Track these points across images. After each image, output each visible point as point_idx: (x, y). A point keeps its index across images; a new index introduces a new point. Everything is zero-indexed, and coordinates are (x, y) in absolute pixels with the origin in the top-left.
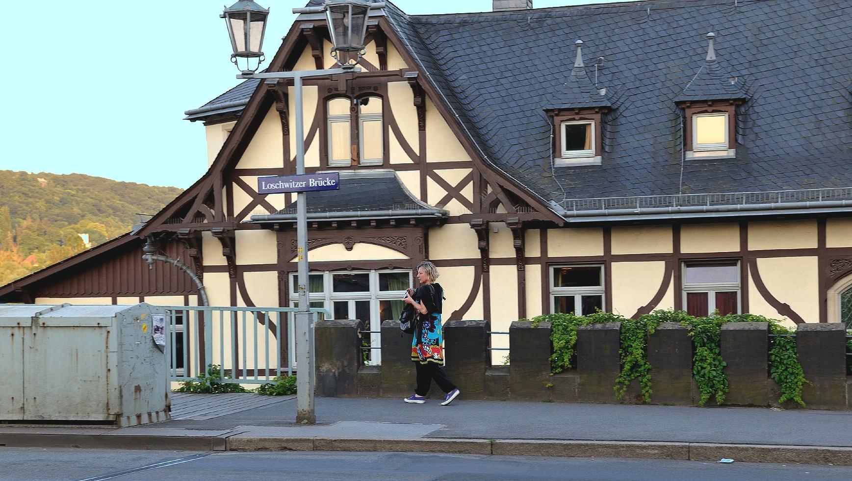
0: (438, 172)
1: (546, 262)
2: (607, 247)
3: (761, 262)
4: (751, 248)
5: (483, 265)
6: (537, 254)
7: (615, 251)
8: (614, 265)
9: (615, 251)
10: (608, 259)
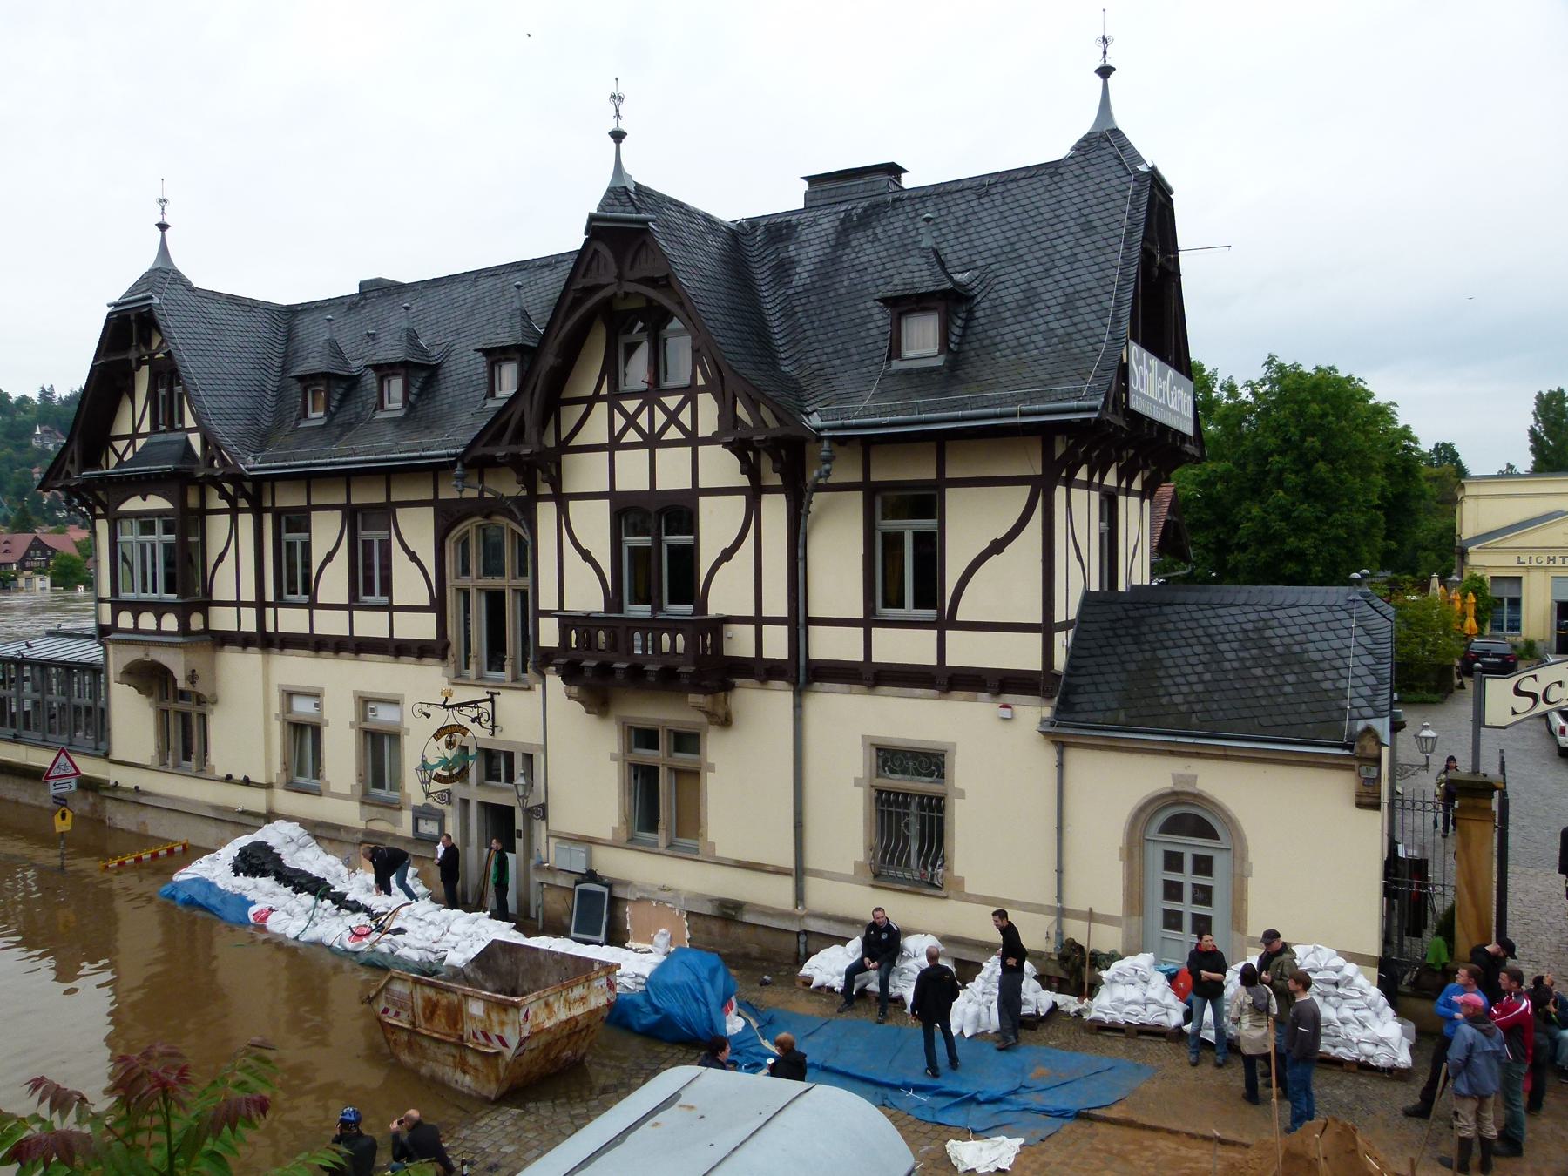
0: (563, 436)
3: (400, 512)
5: (234, 512)
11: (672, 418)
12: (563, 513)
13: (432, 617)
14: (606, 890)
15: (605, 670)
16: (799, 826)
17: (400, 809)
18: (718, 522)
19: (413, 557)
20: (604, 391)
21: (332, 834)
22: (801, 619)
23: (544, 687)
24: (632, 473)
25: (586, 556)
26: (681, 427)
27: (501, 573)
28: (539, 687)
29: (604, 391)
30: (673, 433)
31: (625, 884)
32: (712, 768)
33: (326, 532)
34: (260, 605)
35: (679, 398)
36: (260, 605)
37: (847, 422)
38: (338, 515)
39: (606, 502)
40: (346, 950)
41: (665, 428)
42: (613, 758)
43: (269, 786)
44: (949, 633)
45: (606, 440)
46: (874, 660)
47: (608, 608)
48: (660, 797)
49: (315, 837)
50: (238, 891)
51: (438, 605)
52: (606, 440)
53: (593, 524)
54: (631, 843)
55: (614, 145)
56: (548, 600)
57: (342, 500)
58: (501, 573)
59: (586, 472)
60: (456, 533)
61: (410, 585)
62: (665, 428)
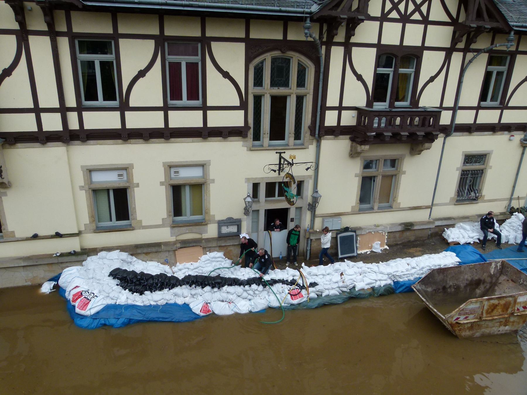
1: (72, 37)
2: (115, 28)
3: (214, 44)
4: (208, 34)
6: (64, 29)
7: (121, 31)
8: (122, 41)
9: (121, 31)
10: (116, 36)
12: (348, 55)
14: (354, 234)
17: (206, 224)
18: (431, 62)
19: (226, 75)
21: (154, 249)
22: (457, 108)
23: (318, 147)
24: (391, 35)
25: (359, 78)
26: (421, 13)
27: (286, 84)
28: (312, 148)
30: (417, 16)
31: (360, 229)
32: (404, 173)
33: (134, 55)
34: (63, 110)
36: (63, 110)
39: (374, 50)
40: (292, 305)
41: (413, 13)
42: (356, 176)
43: (78, 234)
45: (379, 15)
47: (367, 106)
48: (374, 190)
49: (132, 255)
50: (163, 302)
51: (243, 106)
52: (379, 15)
53: (365, 61)
54: (361, 211)
56: (332, 100)
57: (156, 31)
58: (286, 84)
59: (367, 32)
61: (219, 91)
62: (413, 13)
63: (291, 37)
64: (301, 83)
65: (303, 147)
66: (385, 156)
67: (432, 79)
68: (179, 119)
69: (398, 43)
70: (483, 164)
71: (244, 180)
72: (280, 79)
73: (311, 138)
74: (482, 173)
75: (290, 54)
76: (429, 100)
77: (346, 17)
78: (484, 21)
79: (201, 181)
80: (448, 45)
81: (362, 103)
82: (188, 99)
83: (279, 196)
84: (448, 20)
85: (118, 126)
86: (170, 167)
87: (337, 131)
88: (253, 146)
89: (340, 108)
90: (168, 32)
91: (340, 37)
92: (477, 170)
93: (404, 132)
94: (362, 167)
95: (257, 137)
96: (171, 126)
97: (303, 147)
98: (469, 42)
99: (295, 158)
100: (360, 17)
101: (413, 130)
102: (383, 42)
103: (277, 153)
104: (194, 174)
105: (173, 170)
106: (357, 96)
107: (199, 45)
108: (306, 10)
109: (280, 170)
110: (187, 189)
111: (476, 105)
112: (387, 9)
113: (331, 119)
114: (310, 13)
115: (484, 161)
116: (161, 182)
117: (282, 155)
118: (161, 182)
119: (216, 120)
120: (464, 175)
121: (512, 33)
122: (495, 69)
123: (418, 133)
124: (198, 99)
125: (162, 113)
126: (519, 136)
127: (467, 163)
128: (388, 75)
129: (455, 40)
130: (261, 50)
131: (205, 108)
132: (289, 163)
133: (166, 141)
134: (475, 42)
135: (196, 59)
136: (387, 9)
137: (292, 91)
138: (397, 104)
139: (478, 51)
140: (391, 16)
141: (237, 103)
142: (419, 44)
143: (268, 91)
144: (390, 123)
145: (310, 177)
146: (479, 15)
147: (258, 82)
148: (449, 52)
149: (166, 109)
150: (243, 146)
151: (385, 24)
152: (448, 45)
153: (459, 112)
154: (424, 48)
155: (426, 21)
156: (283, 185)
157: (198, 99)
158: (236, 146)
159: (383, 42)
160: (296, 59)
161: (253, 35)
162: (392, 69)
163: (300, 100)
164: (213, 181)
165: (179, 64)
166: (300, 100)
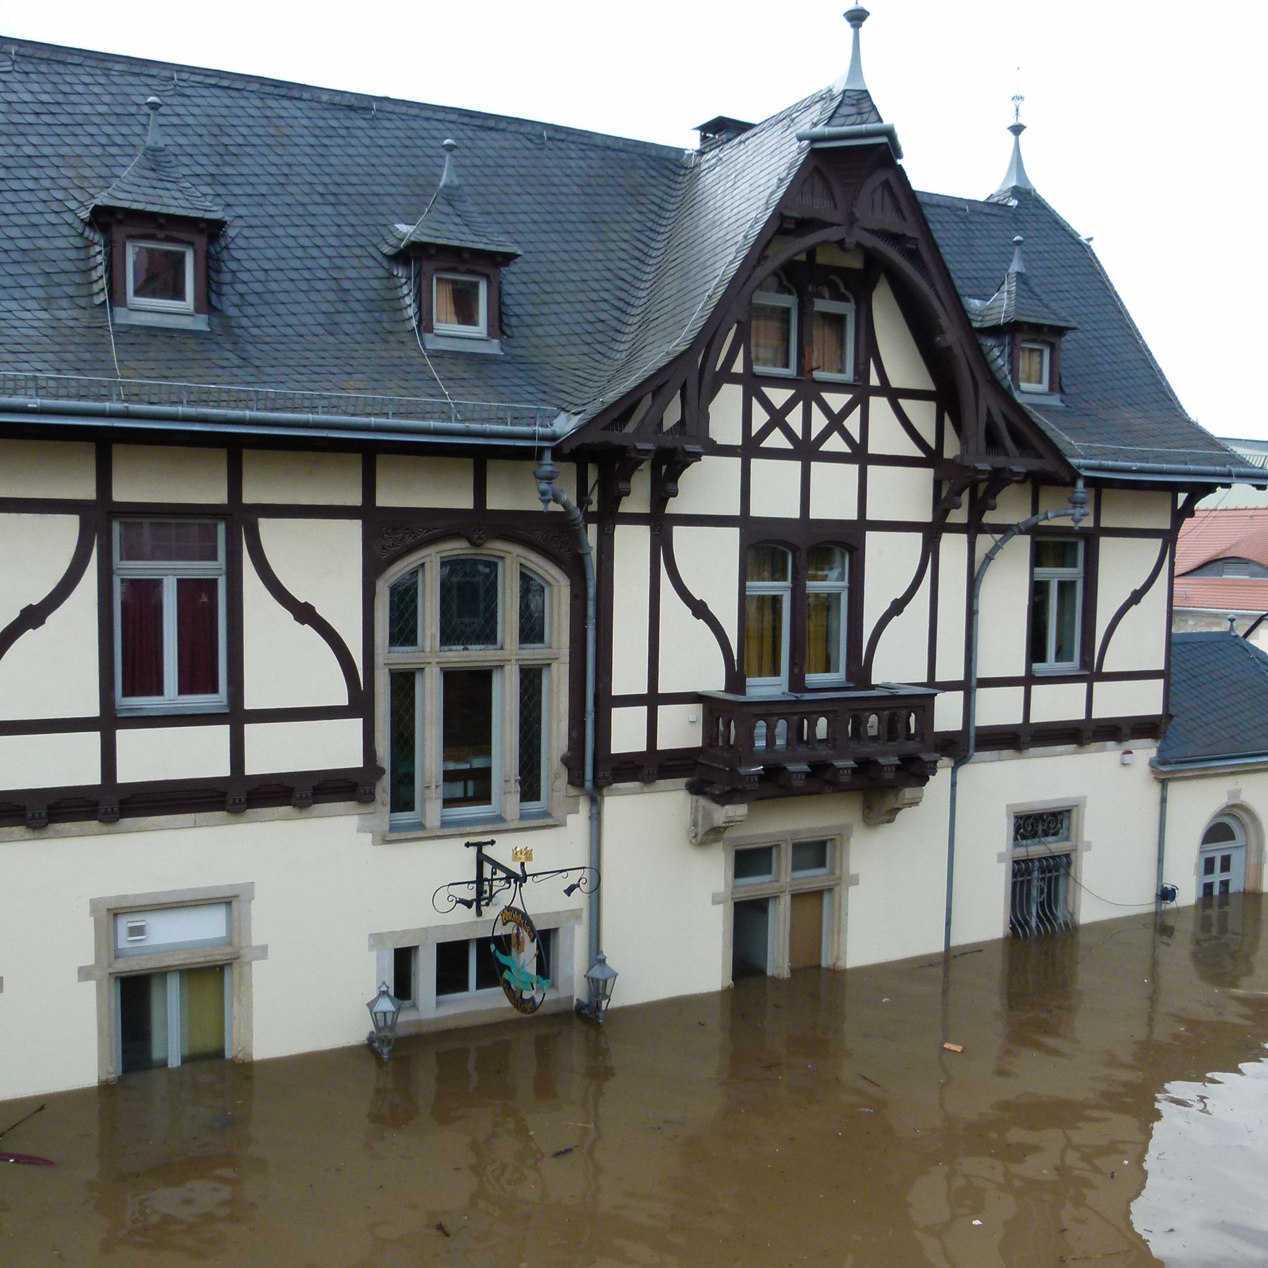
3: (268, 528)
11: (836, 422)
12: (662, 547)
13: (355, 726)
15: (865, 767)
16: (948, 924)
18: (889, 563)
19: (305, 613)
20: (738, 367)
22: (974, 682)
23: (596, 819)
24: (776, 491)
25: (700, 610)
27: (488, 635)
28: (578, 822)
29: (738, 367)
30: (835, 443)
32: (855, 880)
35: (846, 398)
37: (1105, 463)
38: (70, 526)
39: (734, 533)
41: (825, 435)
42: (716, 900)
44: (1096, 685)
45: (738, 441)
46: (1094, 717)
51: (360, 704)
52: (738, 441)
53: (711, 562)
55: (851, 31)
56: (628, 675)
57: (85, 490)
58: (488, 635)
59: (708, 485)
60: (398, 571)
61: (282, 661)
62: (825, 435)
63: (495, 502)
64: (531, 631)
65: (549, 821)
66: (794, 833)
67: (897, 607)
68: (148, 756)
69: (796, 514)
70: (1067, 839)
71: (365, 943)
72: (467, 620)
73: (573, 791)
74: (1069, 864)
75: (497, 547)
76: (896, 663)
77: (650, 446)
78: (1007, 454)
79: (218, 956)
80: (926, 516)
81: (713, 680)
82: (183, 690)
83: (479, 986)
84: (918, 453)
85: (93, 777)
86: (113, 913)
87: (651, 767)
88: (393, 828)
89: (653, 699)
90: (122, 493)
91: (637, 500)
92: (1053, 858)
93: (843, 758)
94: (731, 873)
95: (403, 800)
96: (1033, 720)
97: (549, 821)
98: (978, 508)
99: (529, 858)
100: (690, 448)
101: (867, 750)
102: (755, 512)
103: (468, 845)
104: (194, 932)
105: (124, 924)
106: (696, 663)
107: (221, 529)
108: (540, 430)
109: (482, 898)
110: (173, 984)
111: (1021, 672)
112: (756, 428)
113: (627, 732)
114: (553, 438)
115: (1068, 829)
116: (81, 969)
117: (487, 850)
118: (81, 969)
119: (271, 752)
120: (1021, 872)
121: (1080, 484)
122: (1053, 575)
123: (881, 761)
124: (215, 690)
125: (93, 739)
126: (1145, 751)
127: (1024, 837)
128: (776, 601)
129: (941, 505)
130: (409, 541)
131: (237, 717)
132: (511, 876)
133: (104, 828)
134: (993, 508)
135: (214, 569)
136: (756, 428)
137: (506, 655)
138: (813, 679)
139: (1005, 530)
140: (767, 443)
141: (341, 697)
142: (853, 516)
143: (432, 655)
144: (796, 735)
145: (575, 914)
146: (992, 441)
147: (404, 632)
148: (932, 533)
149: (107, 723)
150: (359, 830)
151: (756, 463)
152: (926, 516)
153: (982, 694)
154: (863, 525)
155: (860, 455)
156: (493, 947)
157: (215, 690)
158: (338, 830)
159: (755, 512)
160: (512, 560)
161: (385, 499)
162: (788, 583)
163: (531, 679)
164: (263, 952)
165: (154, 586)
166: (531, 679)
